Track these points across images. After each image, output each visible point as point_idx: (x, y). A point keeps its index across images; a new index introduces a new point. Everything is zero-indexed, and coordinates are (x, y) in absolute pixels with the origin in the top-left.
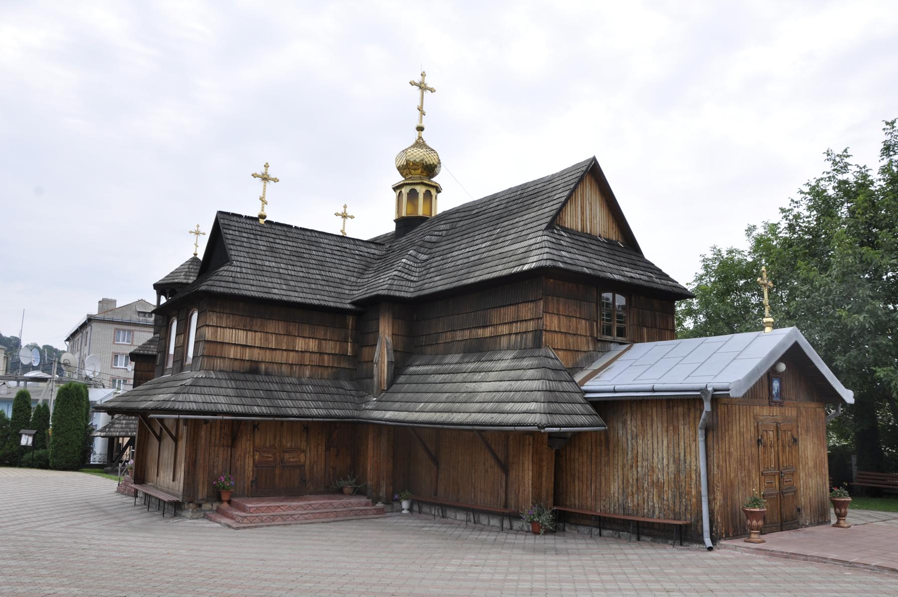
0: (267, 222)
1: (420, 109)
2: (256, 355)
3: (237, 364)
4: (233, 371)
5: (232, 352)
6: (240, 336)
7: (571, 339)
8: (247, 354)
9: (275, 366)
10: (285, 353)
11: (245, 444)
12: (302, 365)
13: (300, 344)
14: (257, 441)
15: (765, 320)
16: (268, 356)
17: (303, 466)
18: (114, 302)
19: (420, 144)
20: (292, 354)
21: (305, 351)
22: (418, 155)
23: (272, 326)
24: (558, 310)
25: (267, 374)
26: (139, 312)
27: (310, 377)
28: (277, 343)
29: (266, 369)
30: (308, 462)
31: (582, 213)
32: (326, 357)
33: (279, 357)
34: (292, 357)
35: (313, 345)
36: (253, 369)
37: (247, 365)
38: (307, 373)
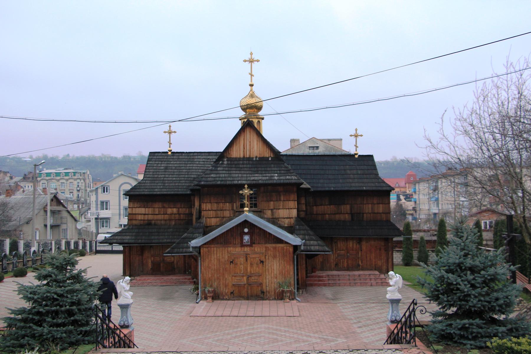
0: (172, 153)
1: (252, 75)
2: (150, 217)
3: (142, 222)
4: (141, 225)
5: (140, 217)
6: (142, 210)
7: (219, 212)
8: (146, 217)
9: (159, 222)
10: (163, 216)
11: (146, 254)
12: (170, 220)
13: (169, 211)
14: (152, 253)
15: (245, 209)
16: (156, 217)
17: (173, 262)
18: (298, 140)
19: (252, 96)
20: (166, 216)
21: (172, 214)
22: (252, 101)
23: (157, 205)
24: (210, 201)
25: (155, 224)
26: (310, 147)
27: (175, 224)
28: (159, 211)
29: (155, 223)
30: (175, 261)
31: (244, 148)
32: (182, 215)
33: (160, 217)
34: (167, 217)
35: (175, 210)
36: (149, 223)
37: (146, 222)
38: (173, 223)
